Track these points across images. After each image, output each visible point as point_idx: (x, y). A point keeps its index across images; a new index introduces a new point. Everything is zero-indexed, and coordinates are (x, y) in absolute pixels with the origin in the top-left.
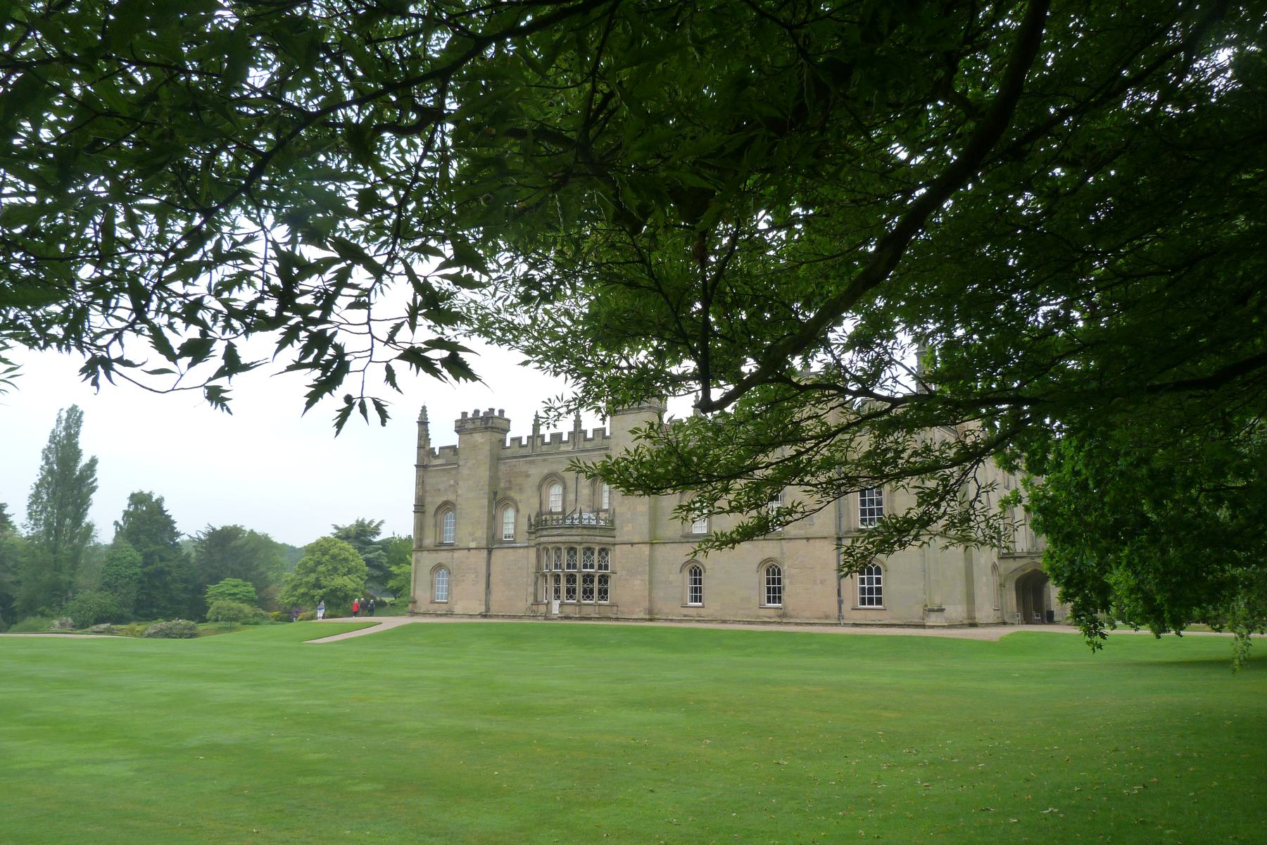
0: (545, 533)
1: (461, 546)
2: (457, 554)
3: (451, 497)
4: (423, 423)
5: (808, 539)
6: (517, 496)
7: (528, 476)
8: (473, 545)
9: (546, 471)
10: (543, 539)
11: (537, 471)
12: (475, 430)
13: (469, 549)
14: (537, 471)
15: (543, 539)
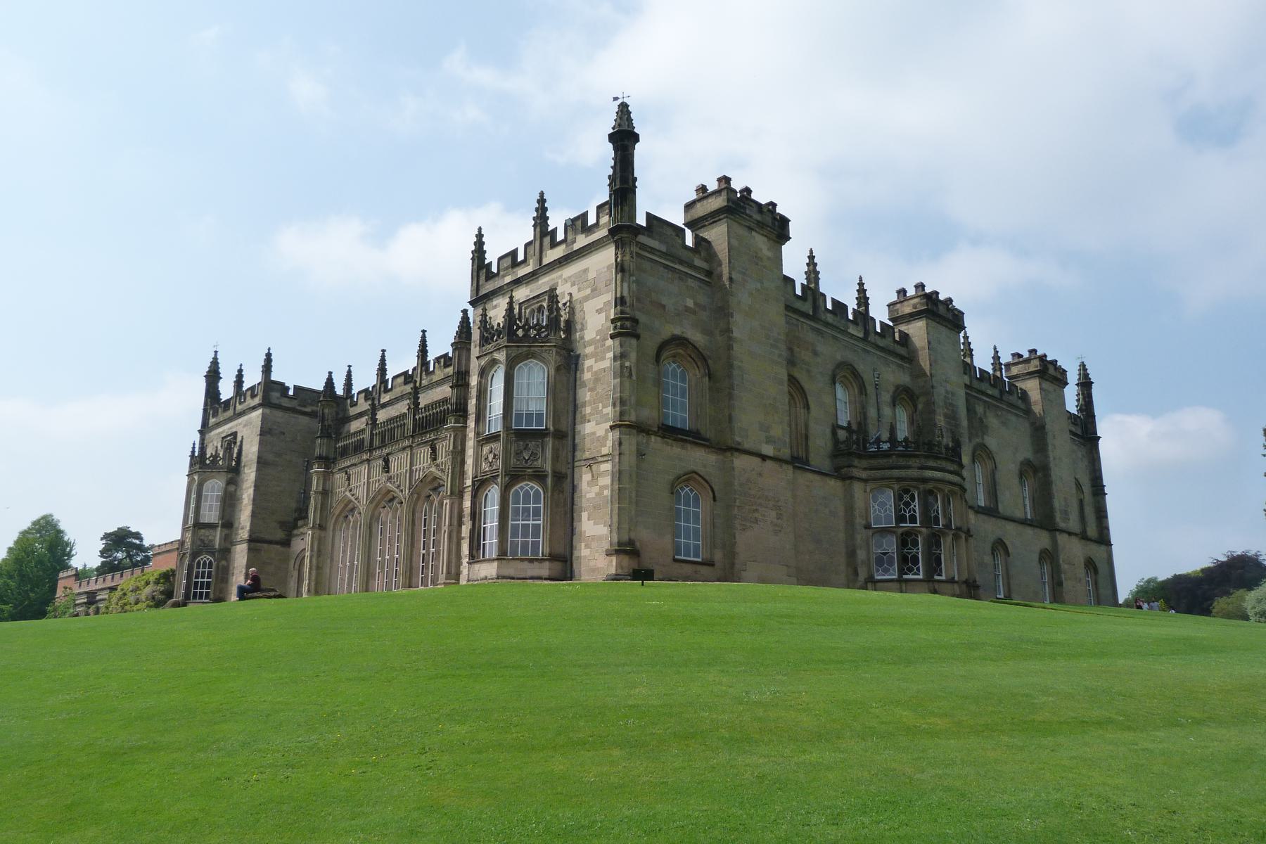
0: (931, 463)
1: (746, 446)
2: (740, 462)
3: (696, 337)
4: (624, 138)
5: (1070, 534)
6: (806, 386)
7: (815, 353)
8: (768, 450)
9: (839, 357)
10: (929, 474)
11: (830, 352)
12: (761, 225)
13: (764, 458)
14: (830, 352)
15: (929, 474)
